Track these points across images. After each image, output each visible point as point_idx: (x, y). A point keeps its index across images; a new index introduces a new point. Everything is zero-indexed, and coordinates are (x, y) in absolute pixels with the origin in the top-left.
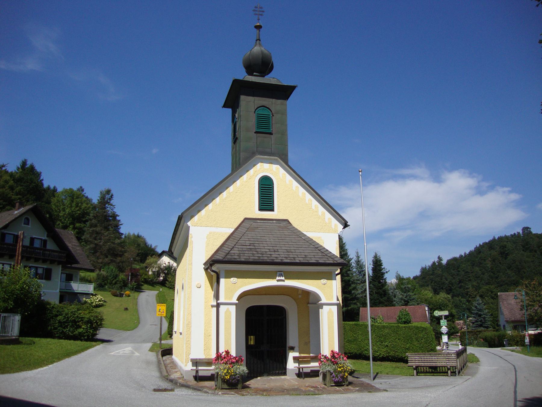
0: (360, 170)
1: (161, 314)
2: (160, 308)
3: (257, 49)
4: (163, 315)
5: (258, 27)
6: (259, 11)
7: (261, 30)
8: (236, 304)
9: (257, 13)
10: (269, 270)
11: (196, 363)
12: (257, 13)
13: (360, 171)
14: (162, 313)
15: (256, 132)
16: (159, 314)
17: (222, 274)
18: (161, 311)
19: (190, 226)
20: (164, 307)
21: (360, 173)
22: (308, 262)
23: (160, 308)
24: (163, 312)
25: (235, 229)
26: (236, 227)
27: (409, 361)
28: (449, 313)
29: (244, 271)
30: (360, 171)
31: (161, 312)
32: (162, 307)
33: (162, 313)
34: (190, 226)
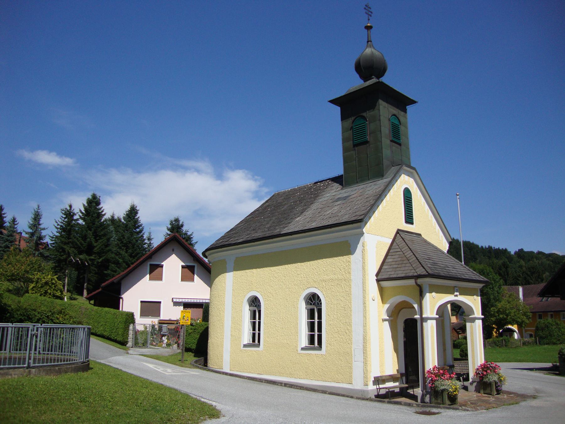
0: (458, 194)
1: (185, 322)
2: (184, 315)
3: (368, 51)
4: (187, 323)
5: (368, 28)
6: (368, 10)
7: (372, 30)
8: (436, 319)
9: (367, 8)
10: (439, 284)
11: (378, 381)
12: (367, 8)
13: (457, 195)
14: (186, 321)
15: (392, 141)
16: (182, 322)
17: (425, 288)
18: (186, 318)
19: (364, 233)
20: (188, 313)
21: (458, 196)
22: (475, 279)
23: (184, 315)
24: (188, 320)
25: (393, 240)
26: (392, 238)
27: (455, 366)
28: (516, 324)
29: (473, 289)
30: (457, 195)
31: (185, 320)
32: (186, 313)
33: (186, 321)
34: (364, 233)
